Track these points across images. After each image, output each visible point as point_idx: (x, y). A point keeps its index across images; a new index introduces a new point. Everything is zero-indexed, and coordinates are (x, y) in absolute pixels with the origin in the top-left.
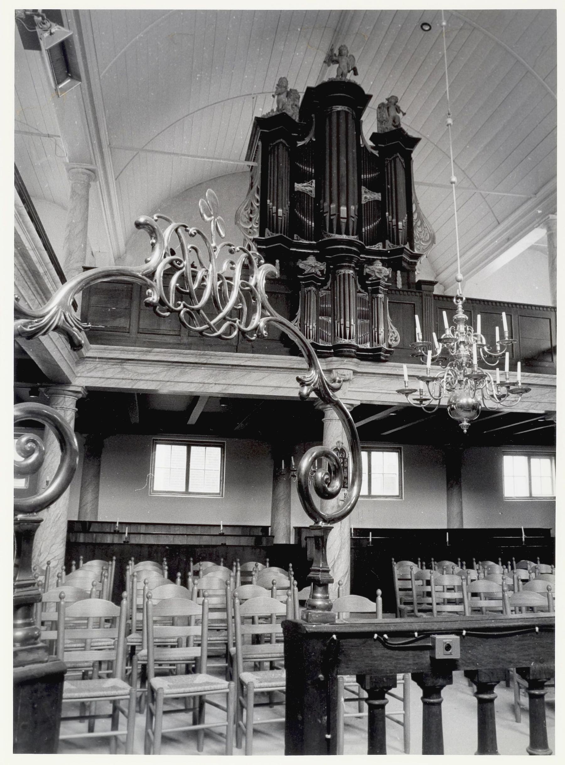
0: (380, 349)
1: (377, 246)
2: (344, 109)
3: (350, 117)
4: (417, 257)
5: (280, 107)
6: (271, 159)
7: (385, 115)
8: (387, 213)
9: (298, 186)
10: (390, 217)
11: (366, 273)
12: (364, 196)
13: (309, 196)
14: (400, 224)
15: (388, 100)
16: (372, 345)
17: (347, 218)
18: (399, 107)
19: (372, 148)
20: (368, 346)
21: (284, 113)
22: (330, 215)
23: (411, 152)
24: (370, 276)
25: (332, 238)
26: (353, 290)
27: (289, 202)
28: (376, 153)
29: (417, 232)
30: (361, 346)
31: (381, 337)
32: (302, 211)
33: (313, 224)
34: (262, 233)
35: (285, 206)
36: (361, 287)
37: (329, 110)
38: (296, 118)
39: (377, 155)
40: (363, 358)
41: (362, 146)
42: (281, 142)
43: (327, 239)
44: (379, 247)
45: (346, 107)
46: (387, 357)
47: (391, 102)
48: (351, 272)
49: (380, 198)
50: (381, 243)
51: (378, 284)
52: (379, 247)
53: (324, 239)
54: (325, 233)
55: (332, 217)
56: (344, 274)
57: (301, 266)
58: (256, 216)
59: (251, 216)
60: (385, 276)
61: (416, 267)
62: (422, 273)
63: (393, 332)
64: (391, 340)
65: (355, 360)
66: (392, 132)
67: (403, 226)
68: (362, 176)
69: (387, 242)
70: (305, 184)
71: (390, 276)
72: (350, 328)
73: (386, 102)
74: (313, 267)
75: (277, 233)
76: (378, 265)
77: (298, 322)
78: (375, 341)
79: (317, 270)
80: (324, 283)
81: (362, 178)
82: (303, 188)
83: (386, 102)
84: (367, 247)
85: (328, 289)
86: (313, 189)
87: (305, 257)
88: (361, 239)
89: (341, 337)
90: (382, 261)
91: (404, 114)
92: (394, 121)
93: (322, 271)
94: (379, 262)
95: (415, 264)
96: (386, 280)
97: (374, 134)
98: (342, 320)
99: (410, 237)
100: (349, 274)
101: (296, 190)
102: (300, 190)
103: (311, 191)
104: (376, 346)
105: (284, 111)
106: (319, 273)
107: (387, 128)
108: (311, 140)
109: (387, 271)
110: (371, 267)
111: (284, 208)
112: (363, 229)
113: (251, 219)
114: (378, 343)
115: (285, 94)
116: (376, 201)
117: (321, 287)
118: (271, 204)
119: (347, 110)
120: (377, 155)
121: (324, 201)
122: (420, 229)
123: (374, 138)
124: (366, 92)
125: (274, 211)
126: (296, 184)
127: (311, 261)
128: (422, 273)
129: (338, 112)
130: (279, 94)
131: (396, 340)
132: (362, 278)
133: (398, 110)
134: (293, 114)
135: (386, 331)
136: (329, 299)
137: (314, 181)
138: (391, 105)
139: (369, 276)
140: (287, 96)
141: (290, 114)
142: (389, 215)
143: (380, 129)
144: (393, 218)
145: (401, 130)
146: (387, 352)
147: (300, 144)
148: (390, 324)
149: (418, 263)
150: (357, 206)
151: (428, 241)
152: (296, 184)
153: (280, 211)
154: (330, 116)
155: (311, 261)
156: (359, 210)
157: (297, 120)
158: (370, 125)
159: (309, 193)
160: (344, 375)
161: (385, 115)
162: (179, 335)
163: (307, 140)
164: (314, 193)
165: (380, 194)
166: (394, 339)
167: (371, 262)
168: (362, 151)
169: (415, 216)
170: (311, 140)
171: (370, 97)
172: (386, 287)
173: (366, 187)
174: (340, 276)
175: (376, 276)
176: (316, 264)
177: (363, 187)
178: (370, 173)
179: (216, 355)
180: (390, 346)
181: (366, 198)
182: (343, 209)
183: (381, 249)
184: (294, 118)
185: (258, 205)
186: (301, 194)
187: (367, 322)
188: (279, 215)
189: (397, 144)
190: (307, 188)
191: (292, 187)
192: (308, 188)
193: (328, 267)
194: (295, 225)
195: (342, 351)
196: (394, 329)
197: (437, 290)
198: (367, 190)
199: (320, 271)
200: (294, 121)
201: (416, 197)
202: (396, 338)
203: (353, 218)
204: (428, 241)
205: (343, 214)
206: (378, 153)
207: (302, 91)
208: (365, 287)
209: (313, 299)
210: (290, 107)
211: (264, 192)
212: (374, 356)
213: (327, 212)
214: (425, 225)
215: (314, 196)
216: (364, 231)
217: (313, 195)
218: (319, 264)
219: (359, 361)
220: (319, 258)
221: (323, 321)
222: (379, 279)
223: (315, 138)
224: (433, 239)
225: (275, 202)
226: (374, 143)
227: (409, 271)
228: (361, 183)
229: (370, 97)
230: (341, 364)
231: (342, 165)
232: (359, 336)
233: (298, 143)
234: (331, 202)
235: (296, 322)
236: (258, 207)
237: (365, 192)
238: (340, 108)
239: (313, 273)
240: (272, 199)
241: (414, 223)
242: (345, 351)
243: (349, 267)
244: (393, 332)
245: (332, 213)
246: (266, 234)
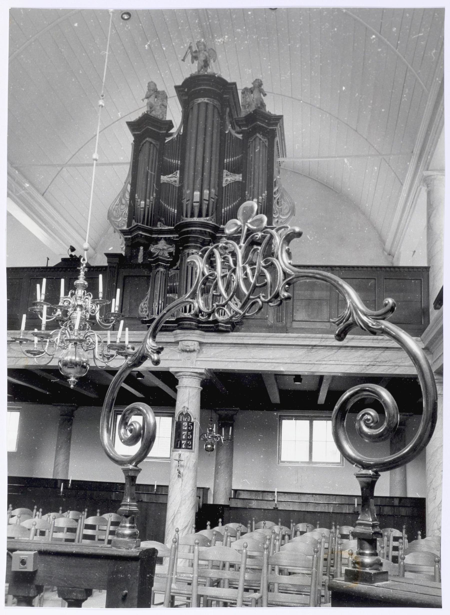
13: (174, 186)
25: (185, 221)
33: (176, 210)
35: (149, 198)
40: (207, 330)
45: (206, 99)
65: (198, 332)
68: (225, 160)
70: (170, 176)
80: (173, 264)
81: (225, 162)
82: (168, 179)
85: (177, 269)
86: (177, 179)
101: (162, 182)
103: (175, 181)
116: (237, 183)
117: (171, 267)
126: (162, 177)
137: (178, 171)
159: (174, 183)
160: (188, 346)
181: (226, 180)
190: (171, 179)
191: (159, 179)
195: (183, 324)
198: (229, 173)
210: (158, 108)
216: (223, 212)
217: (177, 185)
219: (203, 332)
228: (221, 167)
230: (184, 336)
242: (186, 324)
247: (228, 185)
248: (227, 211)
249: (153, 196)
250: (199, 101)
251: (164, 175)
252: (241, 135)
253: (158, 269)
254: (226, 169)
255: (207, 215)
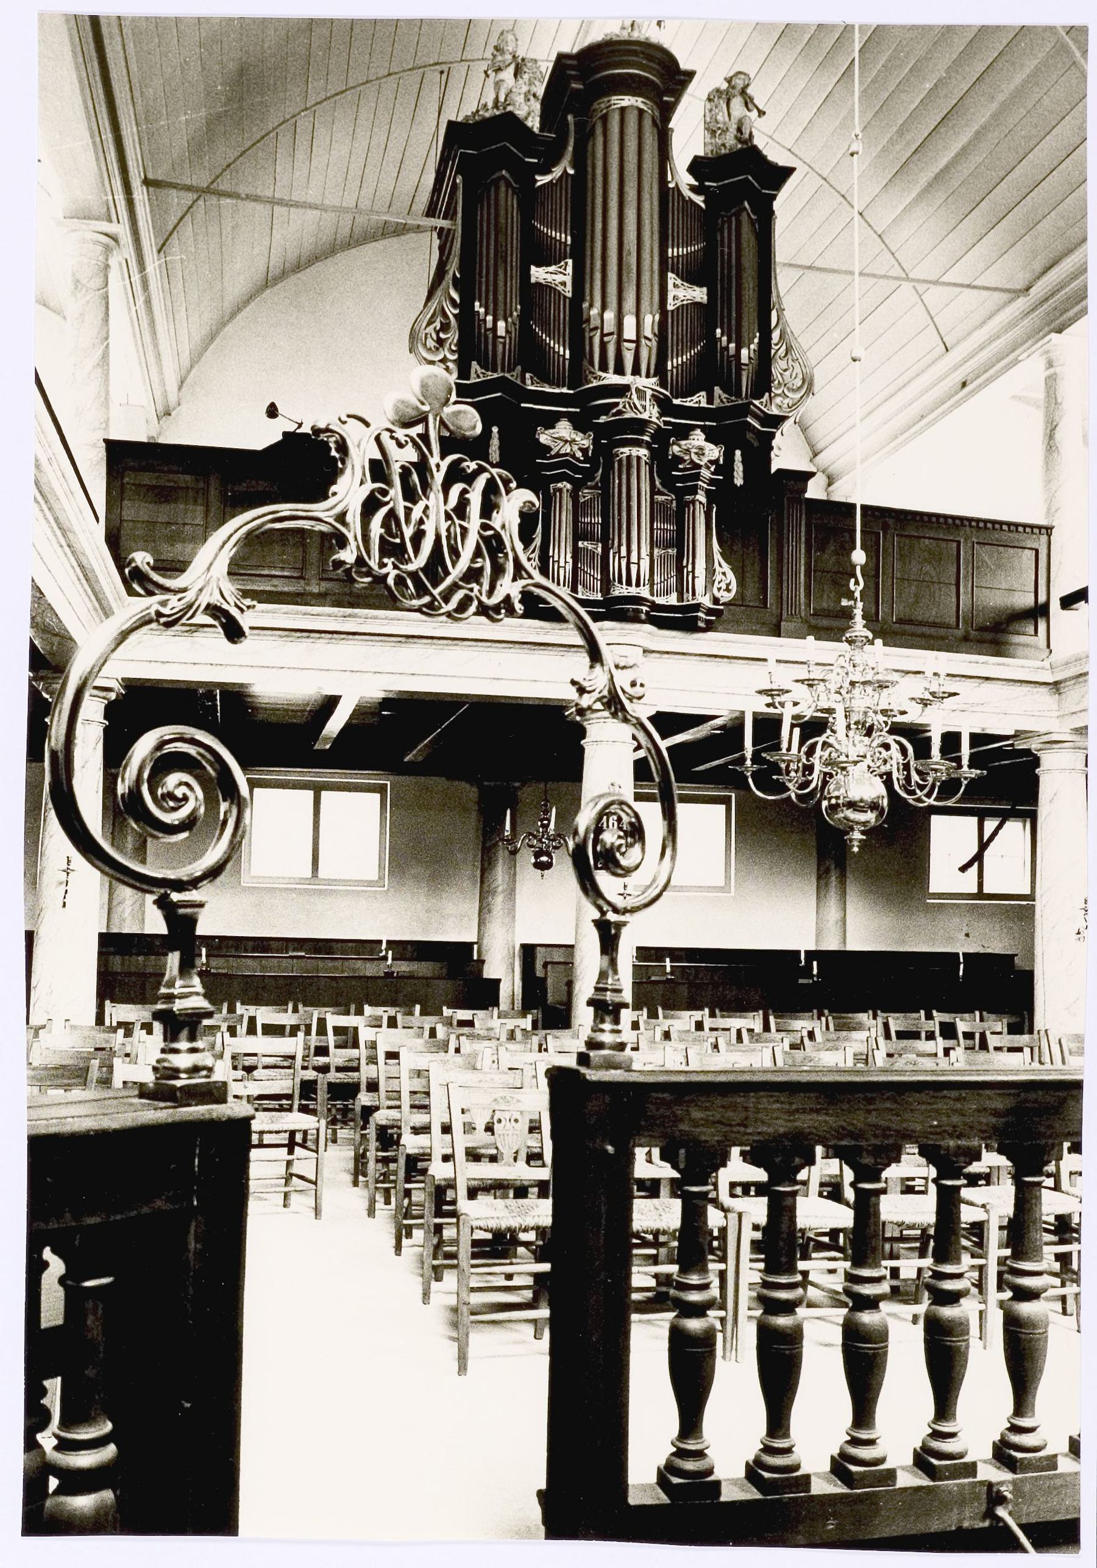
0: (697, 607)
1: (695, 398)
2: (636, 104)
3: (647, 122)
4: (777, 421)
5: (502, 99)
6: (482, 214)
7: (722, 117)
8: (719, 331)
9: (538, 274)
10: (725, 338)
11: (674, 455)
12: (672, 292)
14: (744, 352)
15: (729, 81)
16: (681, 598)
17: (637, 342)
18: (752, 99)
19: (693, 189)
20: (672, 600)
21: (511, 113)
22: (603, 335)
23: (774, 197)
24: (681, 460)
25: (605, 382)
26: (645, 487)
27: (519, 307)
28: (699, 200)
29: (777, 368)
30: (660, 600)
31: (700, 584)
32: (545, 326)
34: (464, 373)
35: (511, 315)
36: (661, 484)
37: (603, 106)
38: (534, 123)
39: (703, 205)
40: (662, 624)
41: (671, 185)
42: (503, 177)
43: (595, 383)
44: (699, 400)
45: (640, 99)
46: (707, 622)
47: (734, 88)
48: (643, 452)
49: (705, 299)
50: (703, 393)
51: (697, 477)
52: (699, 400)
53: (590, 385)
54: (591, 373)
55: (606, 339)
56: (629, 457)
57: (544, 438)
58: (452, 337)
59: (442, 335)
60: (710, 462)
61: (774, 443)
62: (786, 454)
63: (724, 574)
64: (719, 589)
65: (649, 627)
66: (733, 155)
67: (750, 358)
68: (670, 250)
69: (717, 390)
70: (553, 268)
71: (721, 462)
72: (638, 564)
73: (724, 86)
74: (566, 441)
75: (495, 370)
76: (698, 438)
77: (537, 552)
78: (688, 591)
79: (575, 448)
80: (589, 474)
83: (724, 86)
84: (676, 402)
85: (595, 487)
86: (568, 279)
87: (549, 421)
88: (663, 384)
89: (620, 582)
90: (703, 429)
91: (761, 113)
92: (739, 130)
93: (584, 451)
94: (698, 431)
95: (772, 436)
96: (713, 468)
97: (696, 158)
98: (624, 549)
99: (763, 382)
100: (639, 458)
101: (533, 280)
102: (543, 281)
103: (564, 284)
104: (688, 600)
105: (509, 108)
106: (579, 454)
107: (724, 145)
108: (565, 171)
109: (714, 452)
110: (683, 443)
111: (510, 320)
112: (669, 363)
113: (440, 342)
114: (694, 594)
115: (511, 70)
116: (697, 305)
118: (482, 310)
119: (642, 106)
120: (703, 205)
121: (591, 306)
122: (783, 364)
123: (697, 167)
124: (683, 66)
125: (489, 325)
126: (533, 268)
127: (564, 429)
128: (786, 454)
129: (623, 110)
130: (499, 70)
131: (728, 590)
132: (664, 465)
133: (748, 102)
134: (529, 114)
135: (710, 571)
136: (598, 506)
137: (570, 262)
138: (735, 90)
139: (678, 460)
140: (515, 75)
141: (521, 113)
142: (722, 334)
143: (710, 147)
144: (729, 341)
145: (755, 148)
146: (710, 612)
147: (542, 180)
148: (717, 557)
149: (778, 434)
150: (657, 317)
151: (799, 388)
152: (533, 268)
153: (501, 325)
154: (605, 119)
155: (564, 429)
156: (663, 324)
157: (536, 130)
158: (689, 138)
159: (560, 288)
161: (722, 117)
162: (301, 578)
163: (557, 172)
164: (569, 287)
165: (705, 289)
166: (724, 587)
167: (684, 433)
168: (667, 195)
169: (775, 336)
170: (565, 171)
171: (690, 75)
172: (711, 482)
173: (678, 275)
174: (620, 461)
175: (692, 462)
176: (573, 436)
177: (670, 275)
178: (687, 244)
179: (376, 618)
180: (716, 601)
182: (630, 322)
183: (704, 404)
184: (529, 124)
185: (456, 311)
186: (544, 288)
187: (672, 552)
188: (499, 334)
189: (744, 181)
191: (526, 274)
192: (559, 278)
193: (595, 442)
194: (531, 354)
196: (726, 568)
197: (815, 490)
198: (679, 282)
199: (580, 449)
200: (529, 130)
201: (778, 296)
202: (728, 585)
203: (650, 340)
204: (799, 388)
205: (630, 332)
206: (704, 202)
207: (546, 67)
208: (669, 483)
209: (567, 502)
210: (520, 99)
211: (467, 286)
212: (683, 620)
213: (596, 328)
214: (795, 354)
215: (569, 295)
216: (669, 368)
217: (568, 291)
218: (579, 437)
220: (579, 424)
221: (586, 549)
222: (699, 467)
223: (574, 167)
224: (808, 385)
225: (491, 307)
226: (696, 179)
227: (759, 451)
229: (690, 75)
231: (629, 225)
232: (657, 579)
233: (538, 177)
234: (604, 307)
235: (533, 551)
236: (455, 316)
237: (675, 286)
238: (627, 101)
239: (566, 455)
240: (483, 302)
241: (773, 352)
243: (638, 443)
244: (724, 574)
245: (605, 331)
246: (473, 375)
247: (678, 308)
248: (677, 368)
249: (516, 309)
250: (624, 104)
251: (538, 265)
252: (702, 198)
253: (559, 485)
254: (673, 272)
255: (648, 376)
